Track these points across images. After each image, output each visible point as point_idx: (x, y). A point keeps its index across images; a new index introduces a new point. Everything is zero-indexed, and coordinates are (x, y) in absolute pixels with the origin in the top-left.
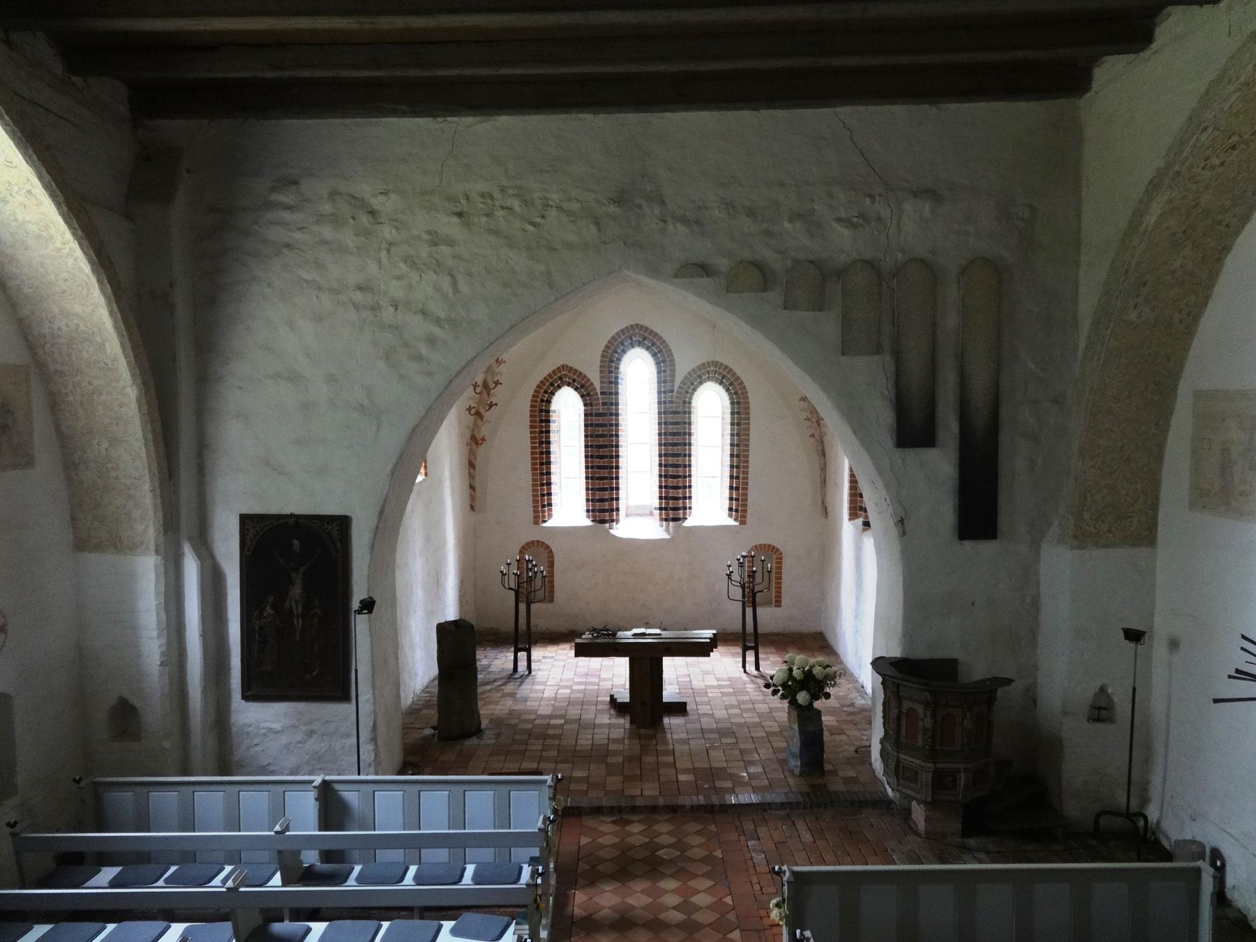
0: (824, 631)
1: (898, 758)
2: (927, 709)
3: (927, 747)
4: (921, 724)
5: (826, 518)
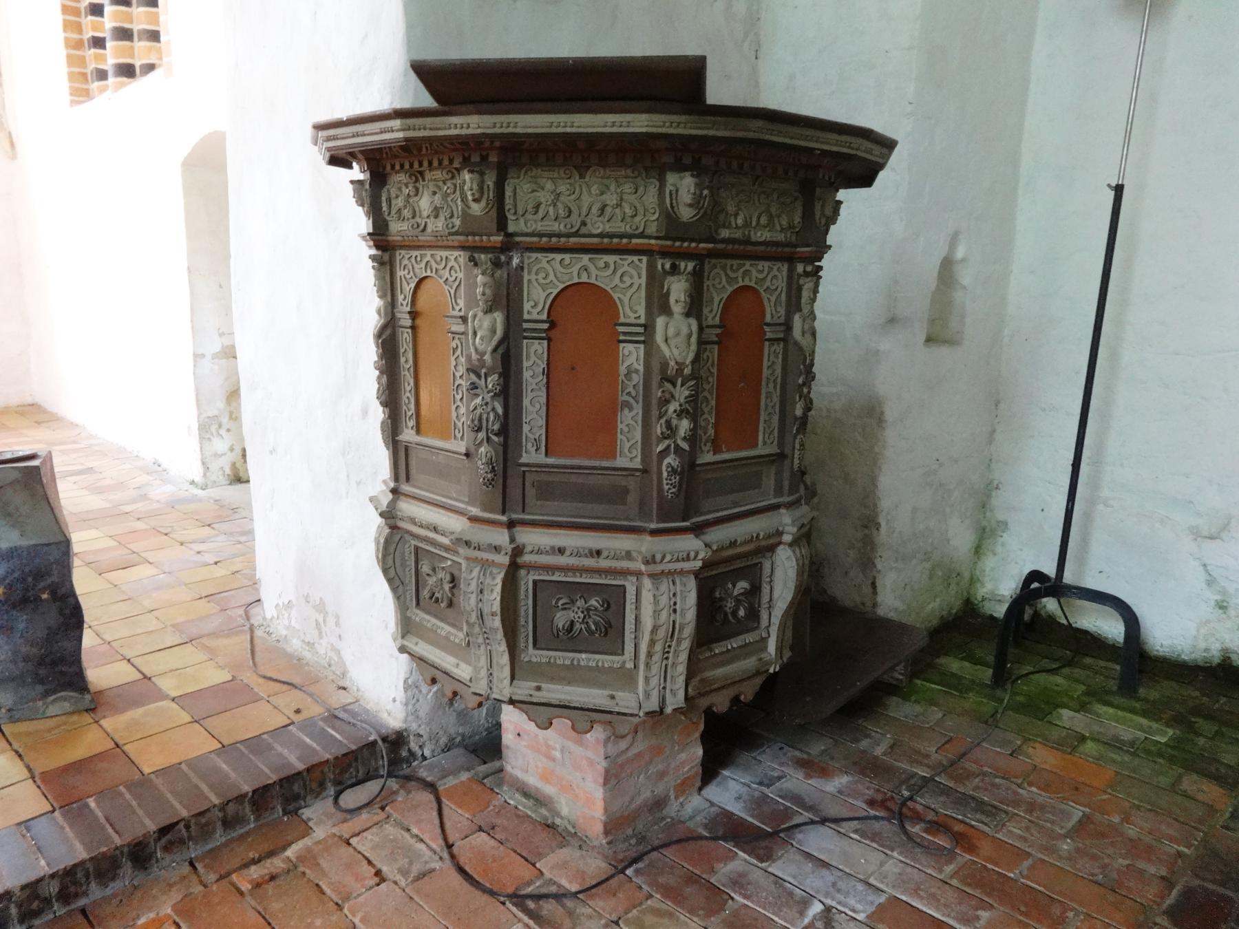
0: (39, 398)
1: (518, 551)
2: (674, 270)
3: (671, 460)
4: (632, 356)
5: (14, 157)
